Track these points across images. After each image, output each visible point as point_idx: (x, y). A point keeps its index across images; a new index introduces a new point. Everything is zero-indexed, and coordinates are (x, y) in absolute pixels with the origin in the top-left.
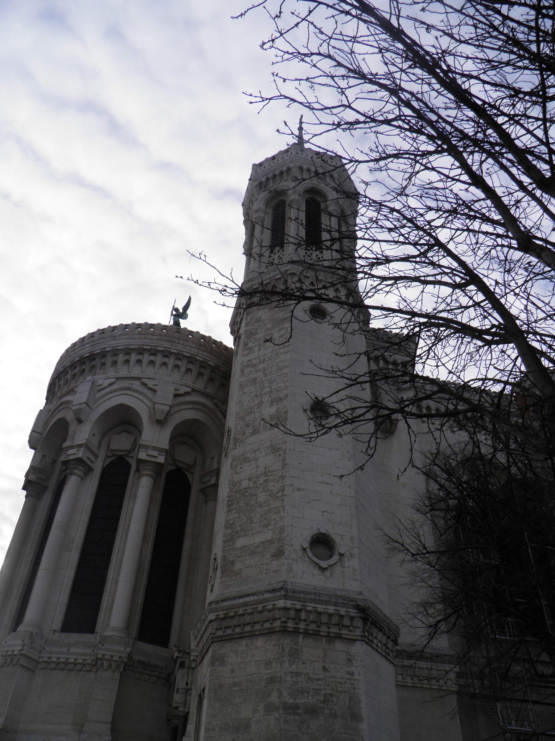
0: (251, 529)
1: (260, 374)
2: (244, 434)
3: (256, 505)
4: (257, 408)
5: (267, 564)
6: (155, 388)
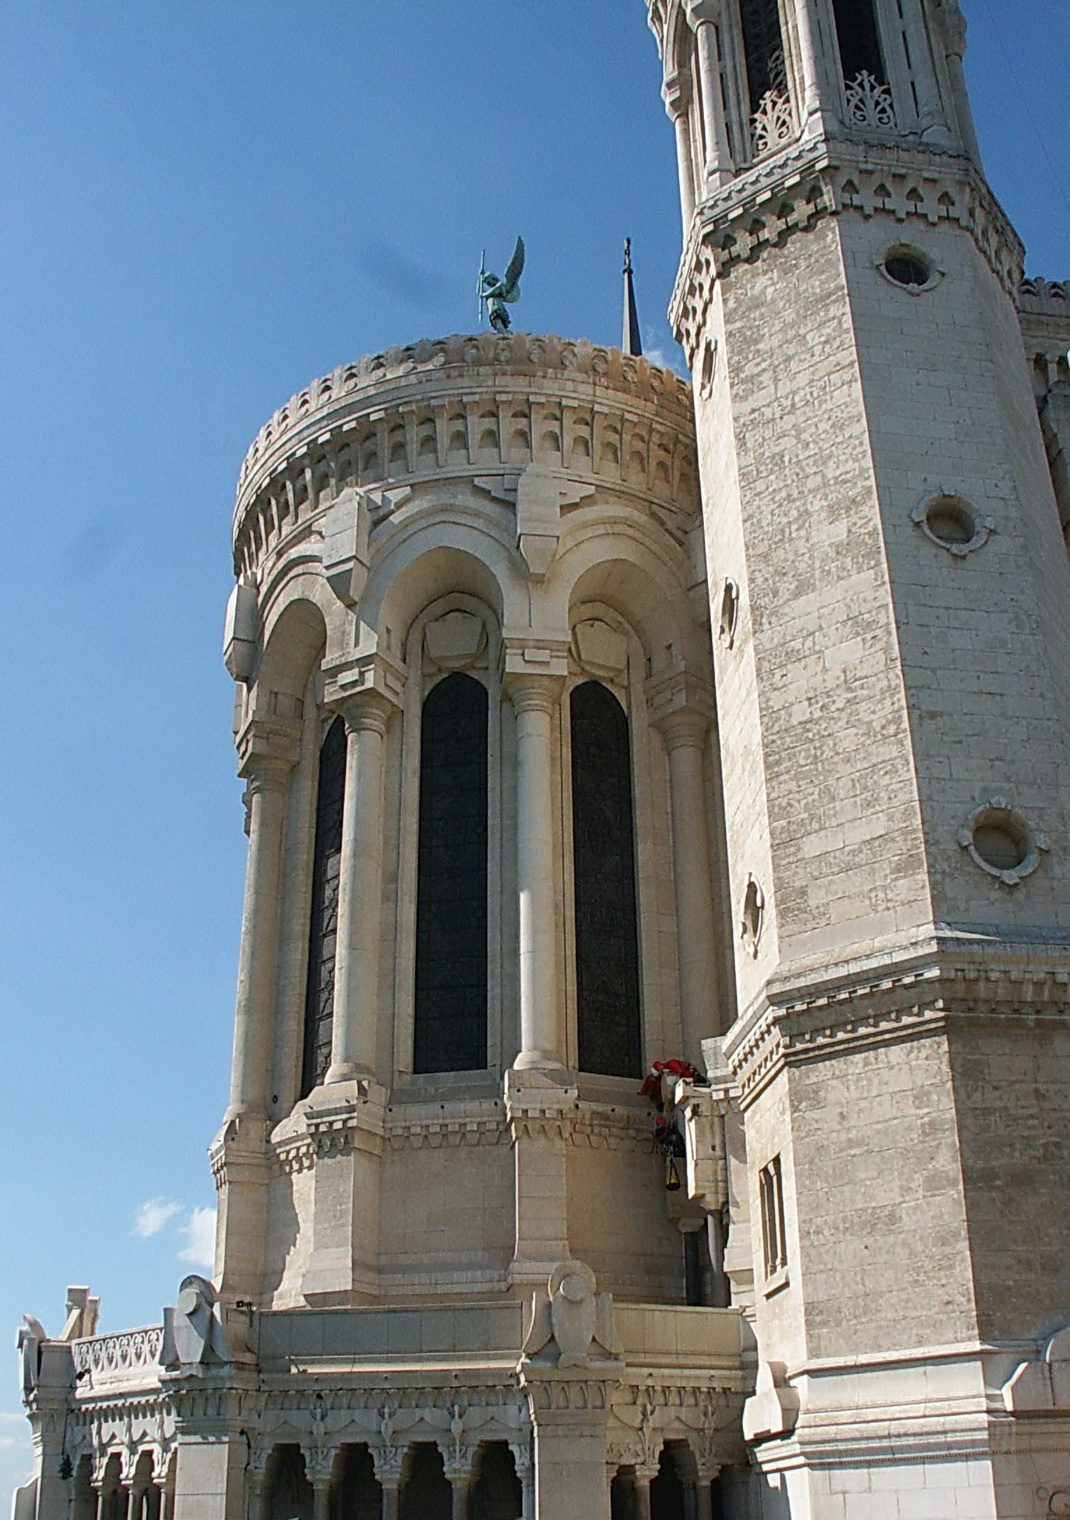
0: (835, 815)
1: (787, 442)
2: (775, 594)
3: (836, 759)
4: (797, 530)
5: (884, 888)
6: (509, 497)
